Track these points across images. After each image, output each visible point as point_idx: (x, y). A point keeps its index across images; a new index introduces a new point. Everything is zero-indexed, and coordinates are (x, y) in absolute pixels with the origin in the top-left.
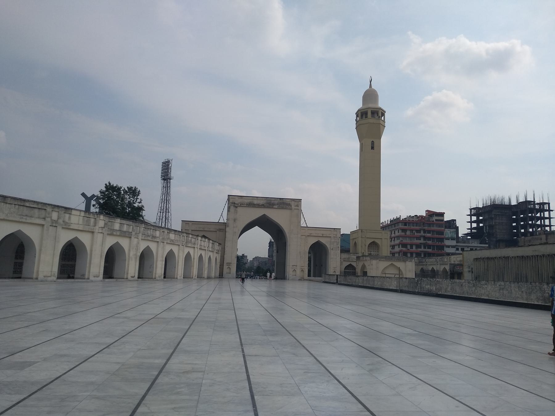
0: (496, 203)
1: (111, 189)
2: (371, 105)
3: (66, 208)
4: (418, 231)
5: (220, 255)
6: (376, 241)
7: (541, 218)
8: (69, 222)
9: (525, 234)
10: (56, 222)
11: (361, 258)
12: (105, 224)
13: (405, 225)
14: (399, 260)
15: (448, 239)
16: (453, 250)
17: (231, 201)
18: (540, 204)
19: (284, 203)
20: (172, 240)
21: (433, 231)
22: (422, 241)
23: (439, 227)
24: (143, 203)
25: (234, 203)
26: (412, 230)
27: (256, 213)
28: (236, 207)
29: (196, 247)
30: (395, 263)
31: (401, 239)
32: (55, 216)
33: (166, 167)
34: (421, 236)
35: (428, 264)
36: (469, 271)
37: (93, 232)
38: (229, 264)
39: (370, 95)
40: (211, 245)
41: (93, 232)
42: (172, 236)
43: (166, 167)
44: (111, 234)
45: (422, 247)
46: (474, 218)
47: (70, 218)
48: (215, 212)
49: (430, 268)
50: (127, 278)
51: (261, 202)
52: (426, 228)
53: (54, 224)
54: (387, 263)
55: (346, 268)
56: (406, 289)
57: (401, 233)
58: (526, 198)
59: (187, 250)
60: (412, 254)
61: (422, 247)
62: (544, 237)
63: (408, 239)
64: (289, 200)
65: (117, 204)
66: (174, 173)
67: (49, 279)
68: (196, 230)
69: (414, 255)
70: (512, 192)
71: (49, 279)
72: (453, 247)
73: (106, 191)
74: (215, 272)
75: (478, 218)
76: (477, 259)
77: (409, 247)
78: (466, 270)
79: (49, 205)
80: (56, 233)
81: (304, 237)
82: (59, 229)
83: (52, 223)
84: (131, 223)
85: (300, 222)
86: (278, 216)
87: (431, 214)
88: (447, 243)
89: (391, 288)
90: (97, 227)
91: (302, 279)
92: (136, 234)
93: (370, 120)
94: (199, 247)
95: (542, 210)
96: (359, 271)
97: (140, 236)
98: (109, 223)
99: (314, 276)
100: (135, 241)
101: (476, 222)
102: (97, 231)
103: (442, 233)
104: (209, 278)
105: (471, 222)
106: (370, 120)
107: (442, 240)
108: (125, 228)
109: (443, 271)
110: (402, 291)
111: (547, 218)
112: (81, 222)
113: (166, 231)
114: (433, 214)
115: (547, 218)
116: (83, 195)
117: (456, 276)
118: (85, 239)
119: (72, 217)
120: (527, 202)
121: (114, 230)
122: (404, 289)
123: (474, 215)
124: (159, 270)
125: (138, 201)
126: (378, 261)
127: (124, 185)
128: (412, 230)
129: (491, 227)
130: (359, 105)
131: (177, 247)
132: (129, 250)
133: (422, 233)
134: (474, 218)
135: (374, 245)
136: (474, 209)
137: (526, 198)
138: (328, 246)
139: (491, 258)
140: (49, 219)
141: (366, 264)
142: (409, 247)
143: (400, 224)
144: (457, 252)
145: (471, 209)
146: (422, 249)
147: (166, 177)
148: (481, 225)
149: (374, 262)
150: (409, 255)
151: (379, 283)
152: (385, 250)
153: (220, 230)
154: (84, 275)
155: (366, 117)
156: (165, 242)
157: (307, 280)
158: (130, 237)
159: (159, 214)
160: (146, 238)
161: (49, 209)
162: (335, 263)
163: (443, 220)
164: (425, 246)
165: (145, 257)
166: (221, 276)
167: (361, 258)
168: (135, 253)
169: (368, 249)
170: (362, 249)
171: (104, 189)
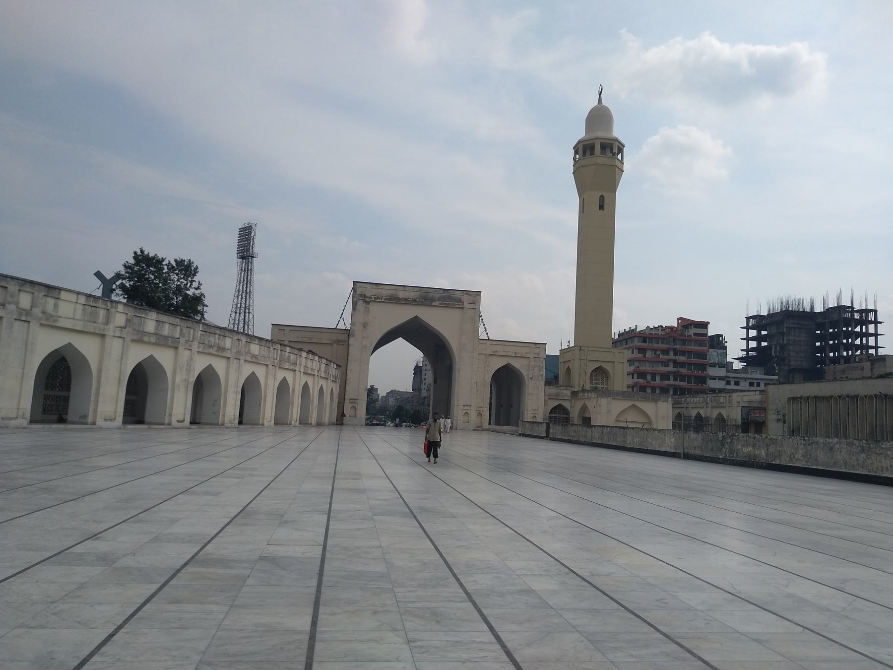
0: (791, 309)
1: (144, 262)
2: (600, 134)
3: (49, 287)
4: (665, 352)
5: (338, 384)
6: (604, 366)
7: (861, 335)
8: (55, 314)
9: (835, 361)
10: (28, 313)
11: (581, 394)
12: (128, 321)
13: (644, 341)
14: (646, 399)
15: (713, 365)
16: (720, 385)
17: (359, 291)
18: (860, 312)
19: (450, 298)
20: (255, 356)
21: (690, 352)
22: (671, 368)
23: (700, 345)
24: (203, 290)
25: (365, 295)
26: (654, 351)
28: (368, 303)
29: (297, 369)
30: (637, 404)
31: (637, 364)
32: (25, 300)
33: (246, 235)
34: (669, 361)
35: (692, 406)
36: (778, 420)
37: (103, 336)
38: (354, 401)
39: (599, 116)
40: (323, 366)
41: (103, 336)
42: (255, 348)
43: (246, 235)
44: (139, 341)
45: (671, 378)
46: (753, 333)
47: (56, 306)
48: (331, 311)
49: (694, 413)
50: (169, 424)
51: (412, 295)
52: (678, 347)
53: (24, 317)
54: (627, 404)
55: (551, 412)
56: (698, 452)
57: (636, 355)
59: (281, 375)
60: (653, 389)
61: (671, 378)
62: (867, 365)
63: (647, 364)
64: (459, 293)
65: (155, 288)
66: (259, 246)
67: (13, 423)
68: (294, 340)
69: (658, 391)
70: (816, 293)
71: (13, 423)
72: (721, 379)
73: (136, 264)
74: (330, 416)
75: (759, 333)
76: (794, 399)
77: (649, 377)
78: (772, 417)
79: (12, 278)
80: (28, 334)
81: (483, 357)
82: (34, 326)
83: (20, 314)
84: (178, 320)
85: (478, 331)
86: (437, 319)
87: (686, 324)
88: (712, 371)
89: (663, 449)
90: (111, 326)
91: (479, 429)
92: (187, 341)
93: (599, 159)
94: (302, 370)
95: (865, 322)
96: (575, 415)
97: (195, 346)
98: (136, 320)
99: (497, 423)
100: (185, 354)
101: (756, 339)
102: (111, 333)
103: (703, 356)
104: (319, 424)
105: (748, 339)
106: (598, 159)
107: (703, 367)
108: (166, 330)
109: (716, 419)
110: (687, 457)
111: (871, 335)
112: (79, 315)
113: (244, 339)
114: (691, 325)
115: (871, 335)
116: (98, 275)
117: (752, 429)
118: (87, 347)
119: (61, 303)
120: (840, 309)
121: (145, 333)
122: (692, 451)
123: (753, 328)
124: (231, 408)
125: (195, 285)
126: (610, 399)
127: (169, 254)
128: (654, 351)
129: (783, 347)
130: (579, 133)
131: (263, 369)
132: (174, 372)
133: (671, 356)
134: (753, 333)
135: (600, 372)
136: (753, 317)
138: (524, 372)
139: (823, 397)
140: (13, 307)
141: (590, 405)
142: (649, 377)
143: (636, 340)
144: (728, 387)
145: (748, 319)
146: (671, 382)
147: (246, 253)
148: (764, 344)
149: (604, 401)
150: (649, 390)
151: (636, 440)
152: (621, 379)
153: (339, 342)
154: (85, 417)
155: (592, 154)
156: (242, 358)
157: (488, 430)
158: (176, 348)
159: (233, 315)
160: (206, 351)
161: (12, 287)
162: (535, 402)
163: (706, 335)
164: (676, 376)
165: (204, 386)
166: (340, 420)
167: (581, 394)
168: (184, 377)
169: (591, 379)
170: (581, 379)
171: (132, 261)
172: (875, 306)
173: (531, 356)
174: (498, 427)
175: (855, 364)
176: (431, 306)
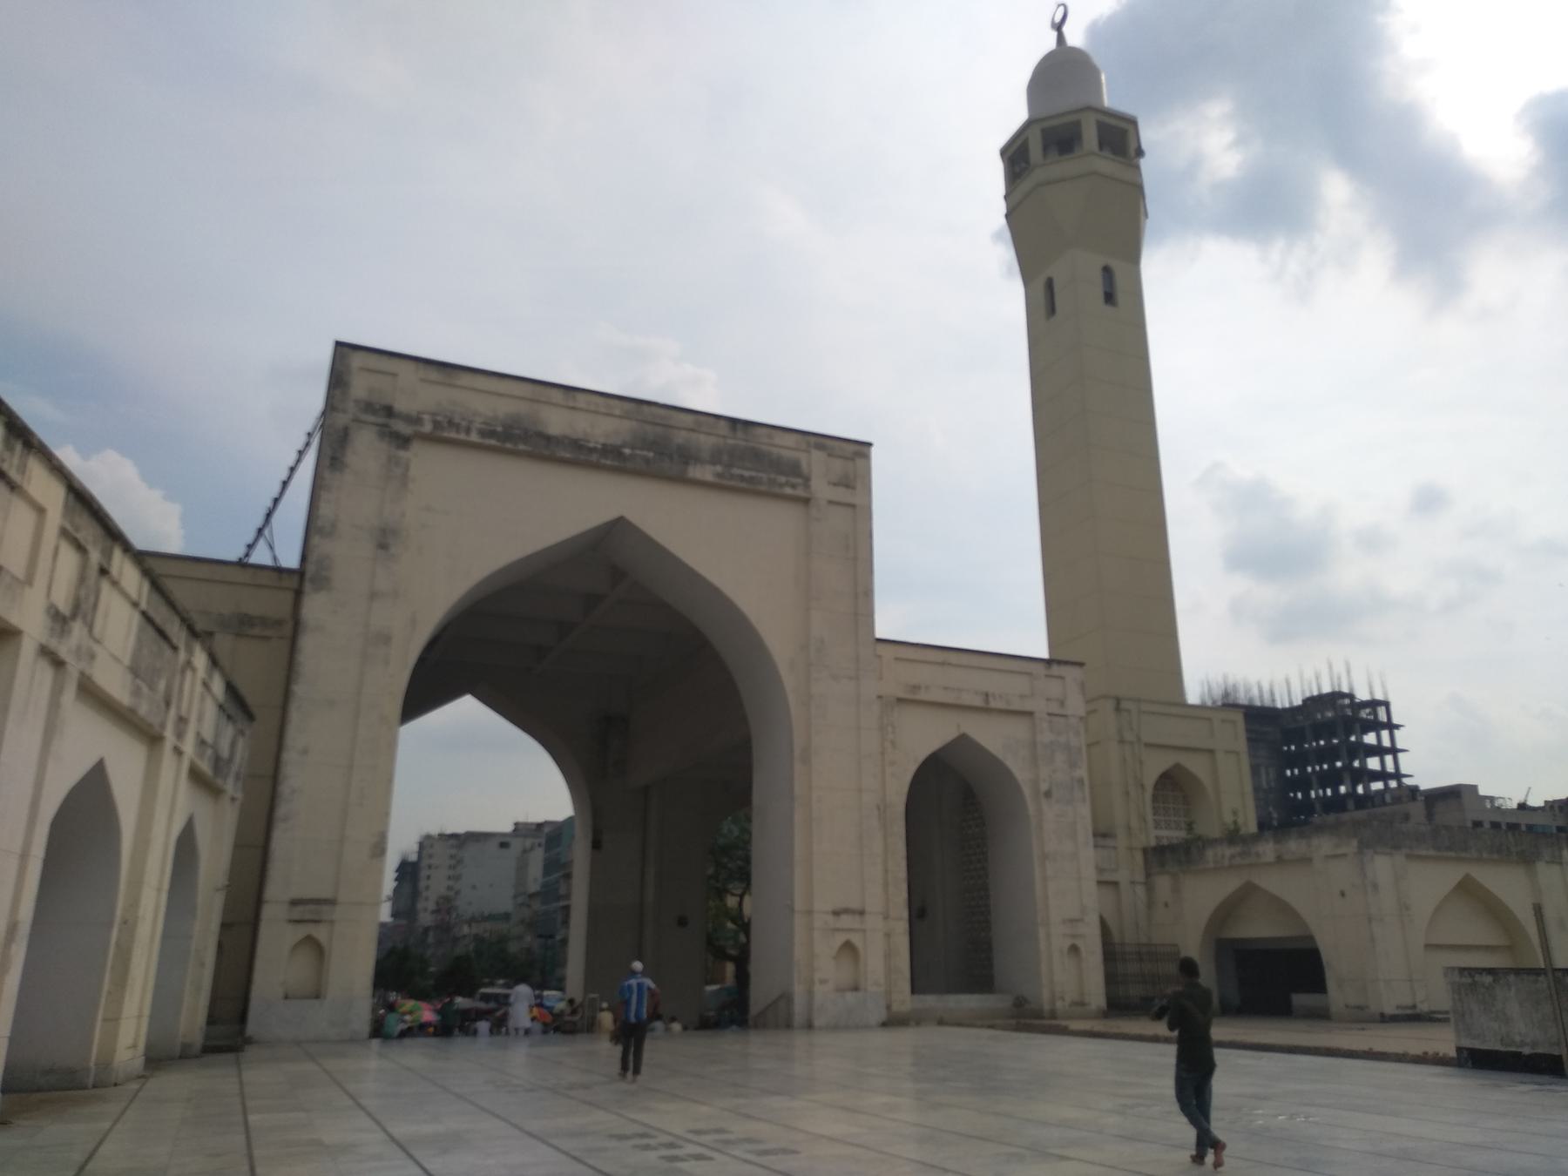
9: (1336, 805)
17: (360, 387)
18: (1365, 704)
19: (757, 457)
25: (379, 408)
27: (555, 509)
28: (403, 441)
51: (601, 430)
58: (1319, 688)
95: (1376, 726)
120: (1336, 696)
135: (1174, 787)
137: (1319, 688)
153: (243, 625)
166: (228, 1029)
172: (1385, 693)
173: (1038, 706)
174: (930, 1001)
175: (1386, 809)
176: (683, 480)
